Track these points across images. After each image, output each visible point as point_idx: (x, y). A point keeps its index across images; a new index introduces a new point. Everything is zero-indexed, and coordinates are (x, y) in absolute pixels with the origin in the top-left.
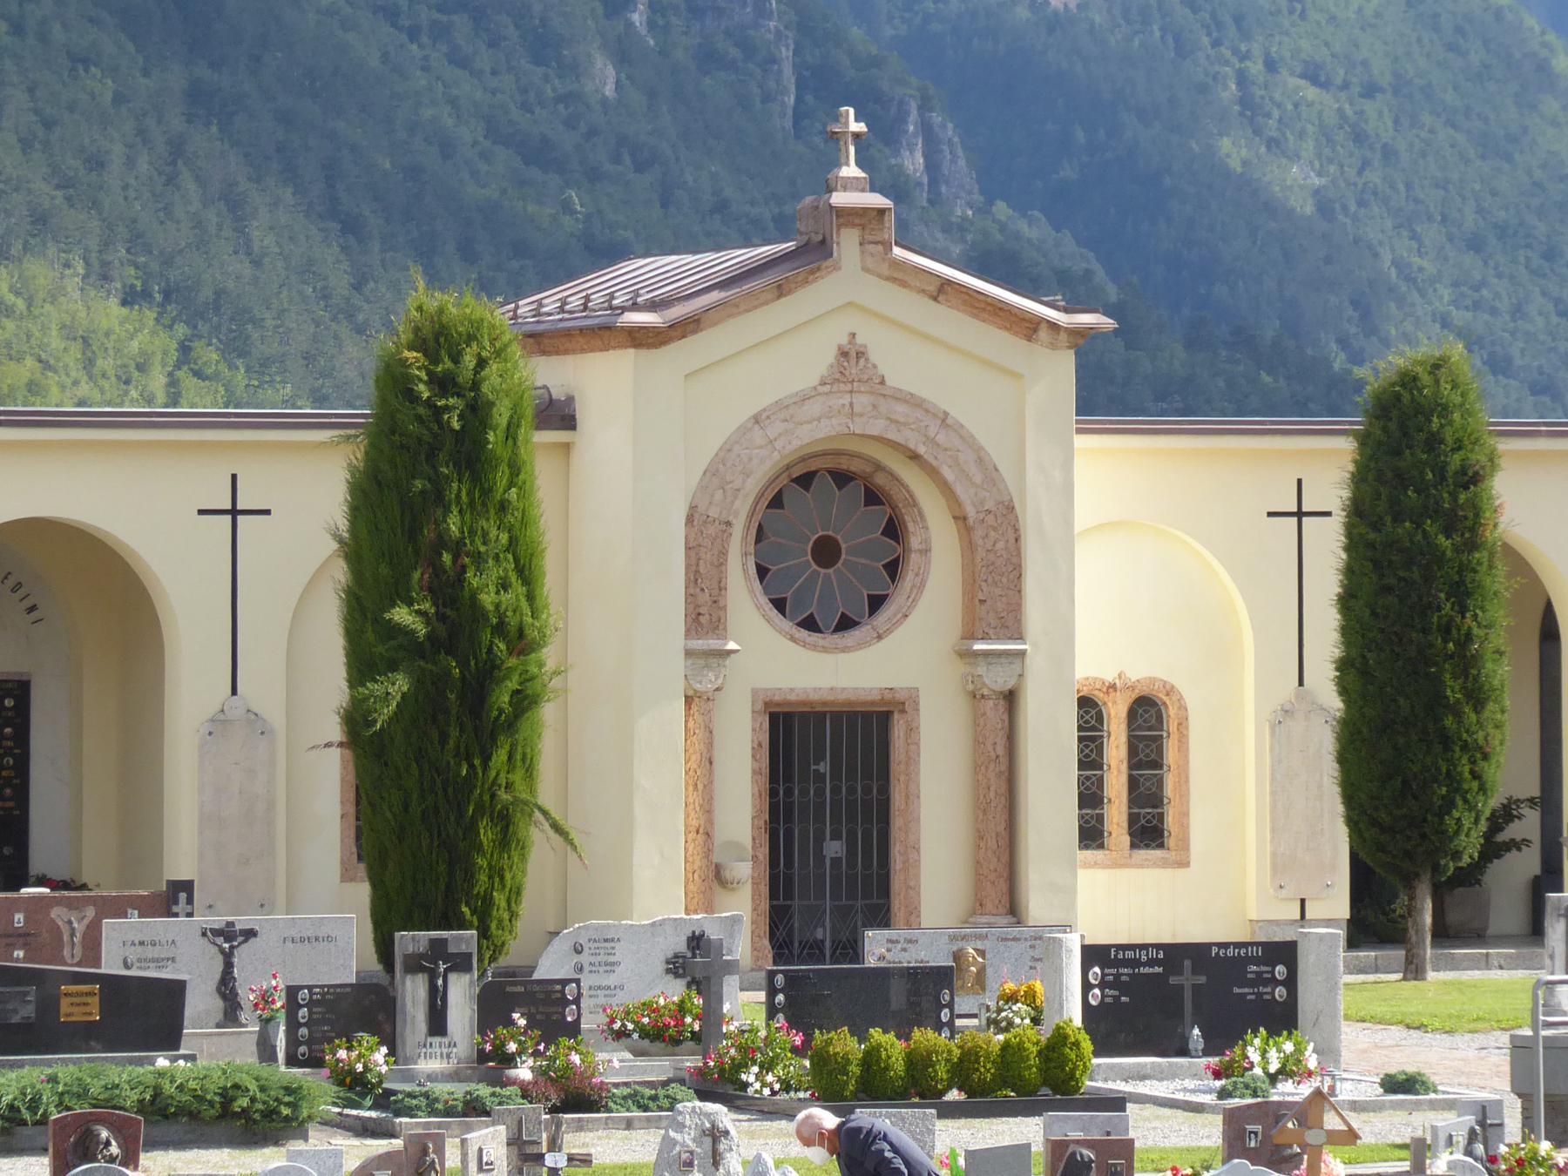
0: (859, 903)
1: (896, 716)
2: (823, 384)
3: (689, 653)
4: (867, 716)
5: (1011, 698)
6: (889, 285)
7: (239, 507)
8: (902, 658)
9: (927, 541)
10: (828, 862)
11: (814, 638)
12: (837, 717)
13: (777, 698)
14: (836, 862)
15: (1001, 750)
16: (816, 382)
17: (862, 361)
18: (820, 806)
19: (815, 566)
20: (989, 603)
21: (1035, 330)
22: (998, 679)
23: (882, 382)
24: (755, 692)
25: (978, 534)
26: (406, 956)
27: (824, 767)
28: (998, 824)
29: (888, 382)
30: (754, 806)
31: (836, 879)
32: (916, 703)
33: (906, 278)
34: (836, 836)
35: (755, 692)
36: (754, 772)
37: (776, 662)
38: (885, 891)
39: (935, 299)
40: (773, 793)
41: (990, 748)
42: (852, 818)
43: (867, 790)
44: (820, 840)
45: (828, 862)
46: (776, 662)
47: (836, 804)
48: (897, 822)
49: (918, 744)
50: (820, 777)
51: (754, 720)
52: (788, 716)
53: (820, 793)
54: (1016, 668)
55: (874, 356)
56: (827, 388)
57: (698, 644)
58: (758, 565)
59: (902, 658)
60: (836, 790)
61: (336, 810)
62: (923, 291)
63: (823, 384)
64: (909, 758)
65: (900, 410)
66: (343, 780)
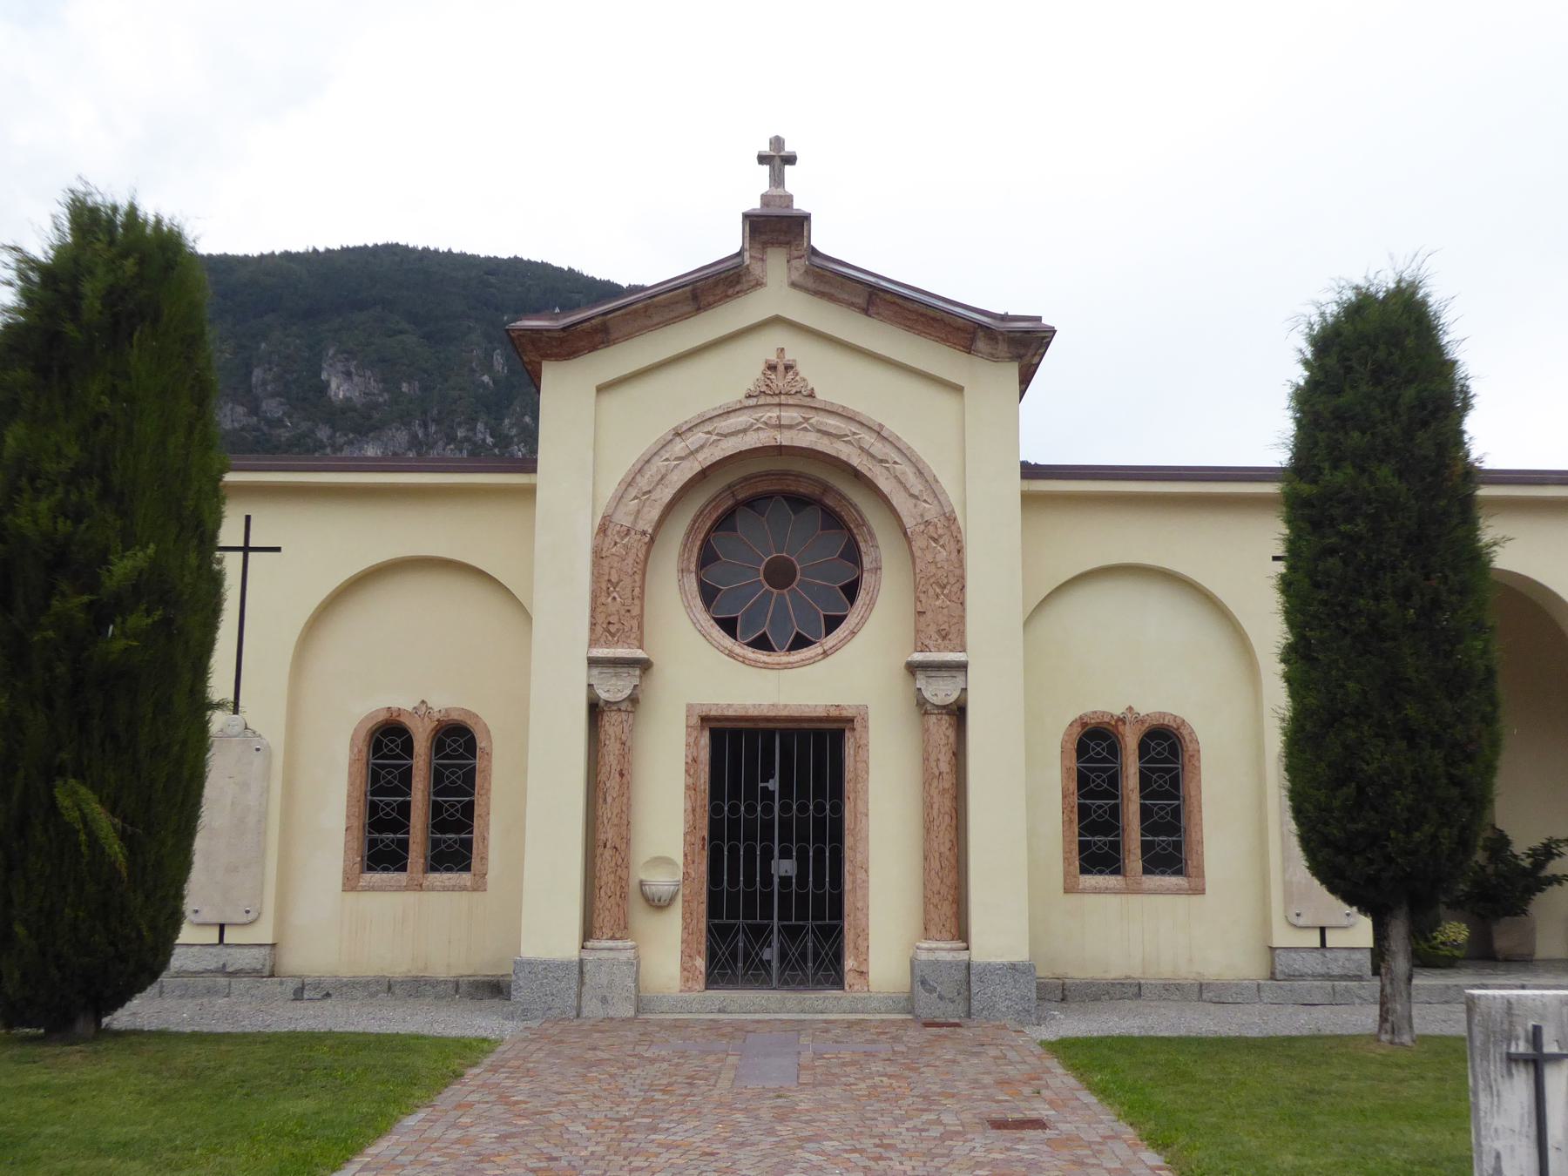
0: (810, 923)
1: (847, 734)
2: (749, 396)
3: (593, 662)
4: (819, 735)
5: (958, 713)
6: (816, 300)
7: (251, 545)
8: (848, 676)
9: (877, 560)
10: (776, 880)
11: (728, 641)
12: (787, 734)
13: (713, 713)
14: (785, 881)
15: (945, 767)
16: (741, 395)
17: (790, 375)
18: (767, 826)
19: (767, 586)
20: (929, 615)
21: (973, 340)
22: (941, 691)
23: (811, 395)
24: (690, 707)
25: (919, 543)
26: (770, 946)
27: (774, 785)
28: (607, 812)
29: (819, 395)
30: (686, 822)
31: (784, 898)
32: (865, 720)
33: (833, 291)
34: (785, 854)
35: (690, 707)
36: (687, 787)
37: (706, 675)
38: (838, 912)
39: (866, 312)
40: (715, 810)
41: (933, 764)
42: (803, 838)
43: (820, 808)
44: (767, 856)
45: (776, 880)
46: (706, 675)
47: (786, 825)
48: (848, 841)
49: (867, 763)
50: (767, 794)
51: (688, 735)
52: (736, 734)
53: (768, 810)
54: (959, 682)
55: (803, 370)
56: (752, 402)
57: (601, 652)
58: (828, 632)
59: (848, 676)
60: (785, 808)
61: (341, 823)
62: (852, 304)
63: (749, 396)
64: (857, 776)
65: (832, 423)
66: (349, 796)
